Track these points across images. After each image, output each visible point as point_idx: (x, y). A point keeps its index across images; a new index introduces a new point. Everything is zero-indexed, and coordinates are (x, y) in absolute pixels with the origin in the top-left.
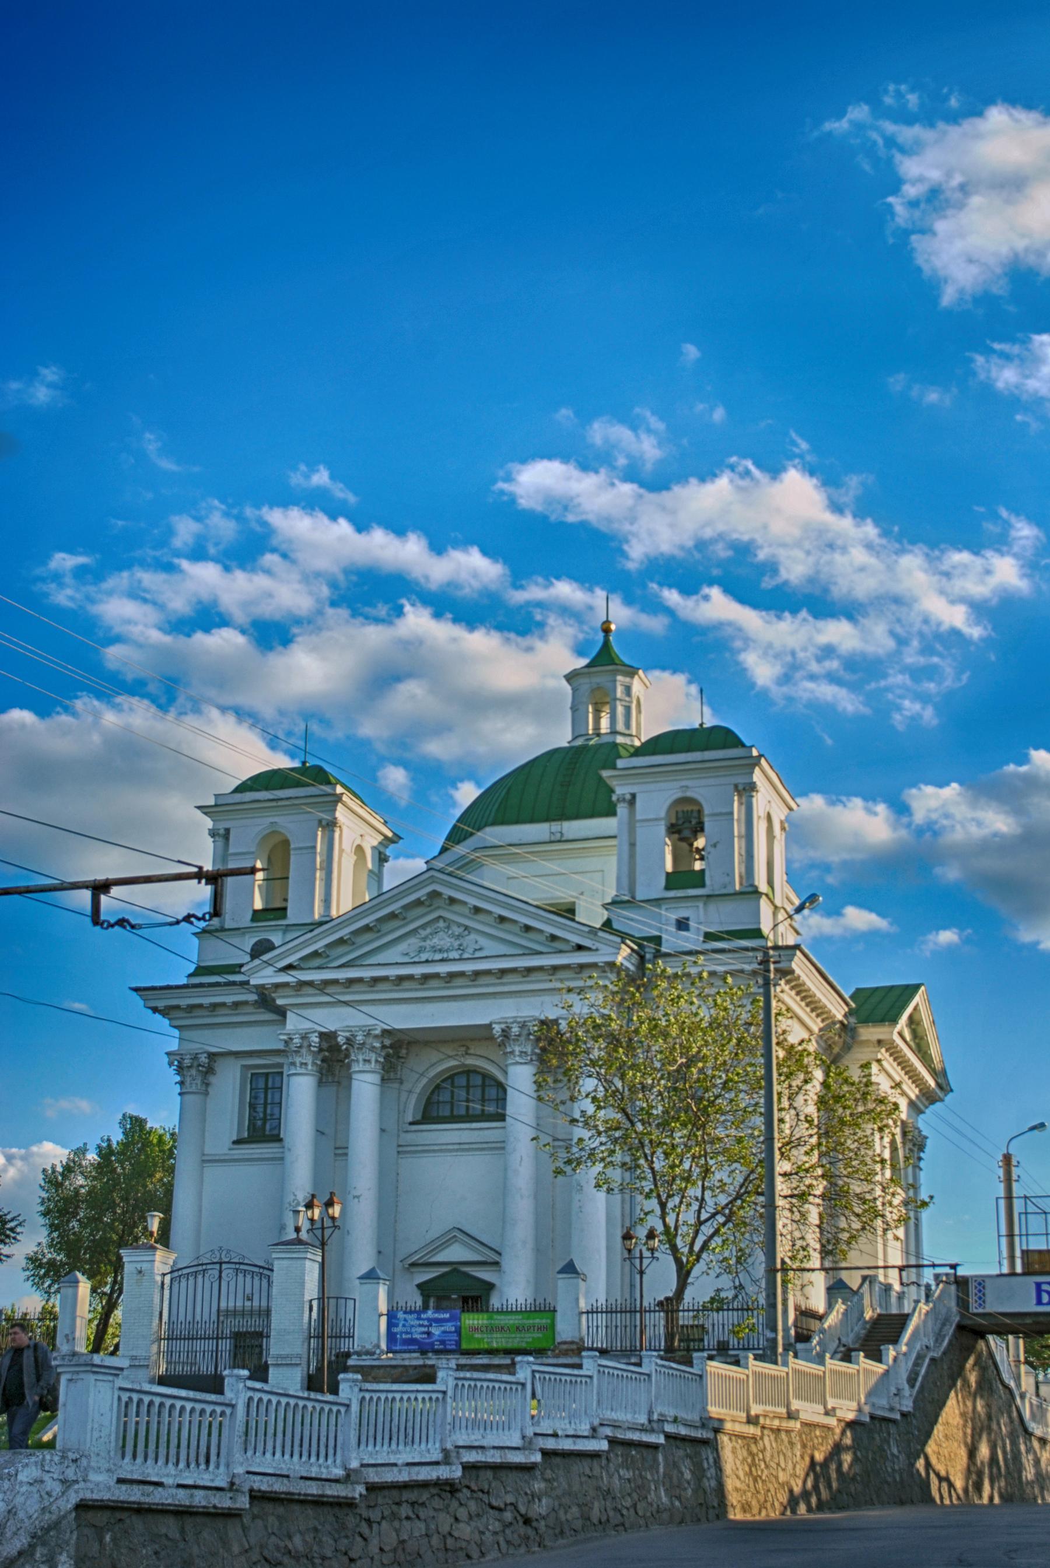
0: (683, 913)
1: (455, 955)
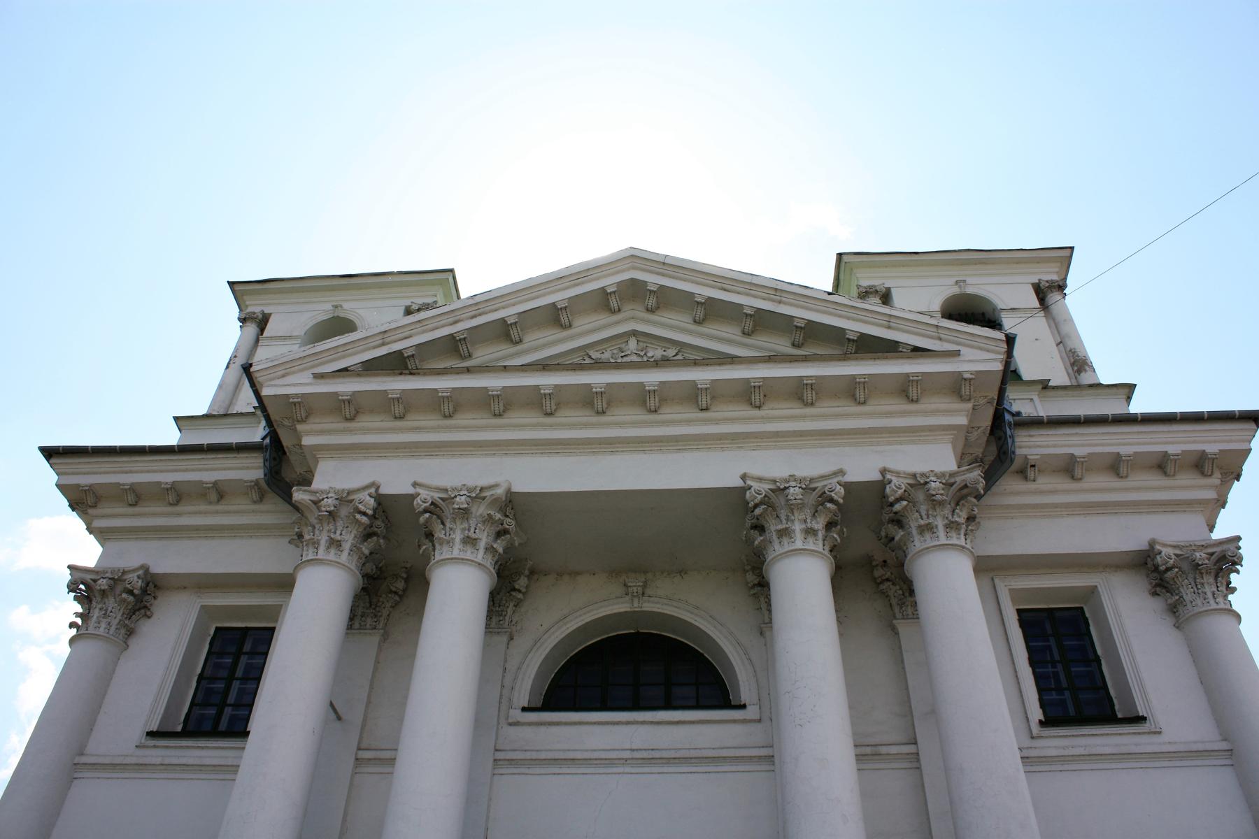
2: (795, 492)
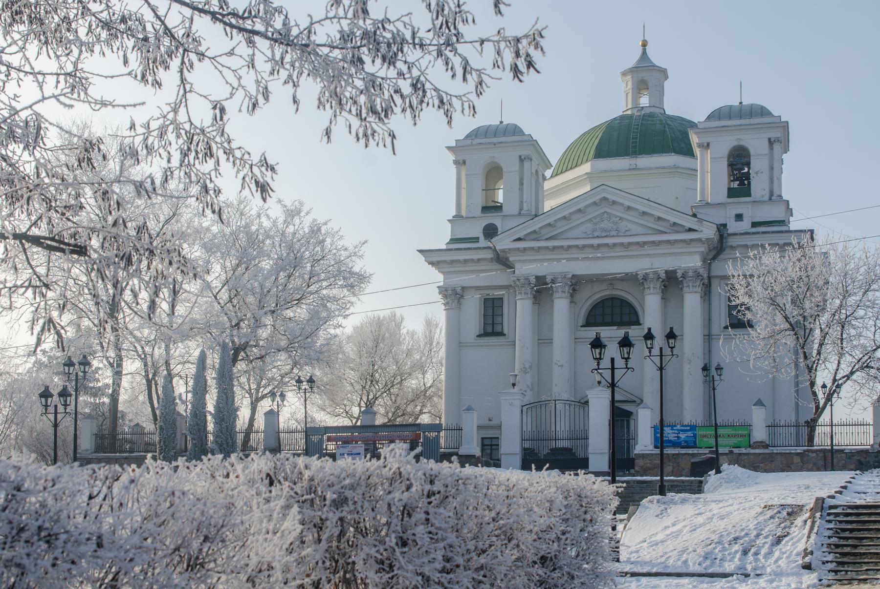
0: (739, 212)
1: (613, 233)
2: (651, 276)
